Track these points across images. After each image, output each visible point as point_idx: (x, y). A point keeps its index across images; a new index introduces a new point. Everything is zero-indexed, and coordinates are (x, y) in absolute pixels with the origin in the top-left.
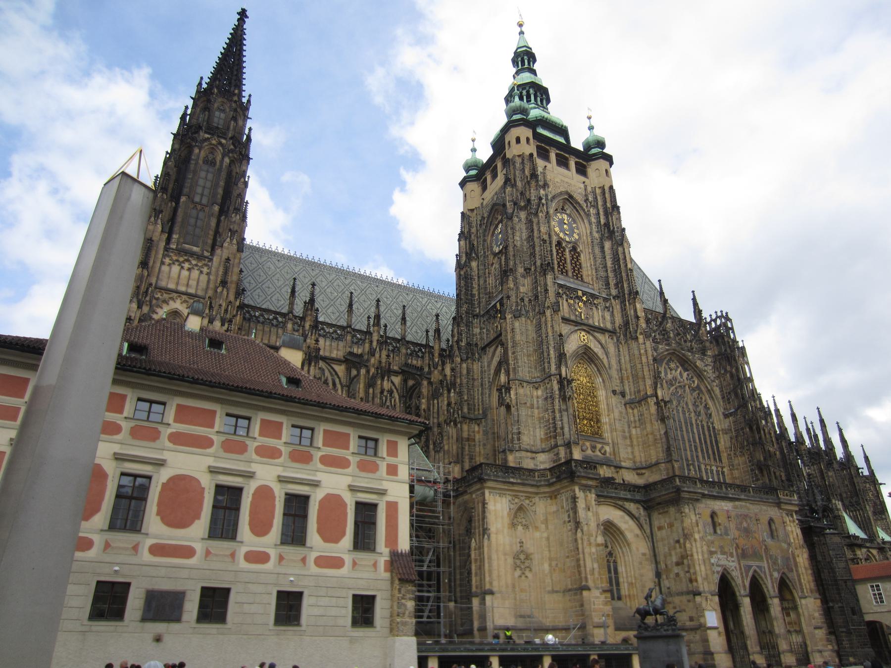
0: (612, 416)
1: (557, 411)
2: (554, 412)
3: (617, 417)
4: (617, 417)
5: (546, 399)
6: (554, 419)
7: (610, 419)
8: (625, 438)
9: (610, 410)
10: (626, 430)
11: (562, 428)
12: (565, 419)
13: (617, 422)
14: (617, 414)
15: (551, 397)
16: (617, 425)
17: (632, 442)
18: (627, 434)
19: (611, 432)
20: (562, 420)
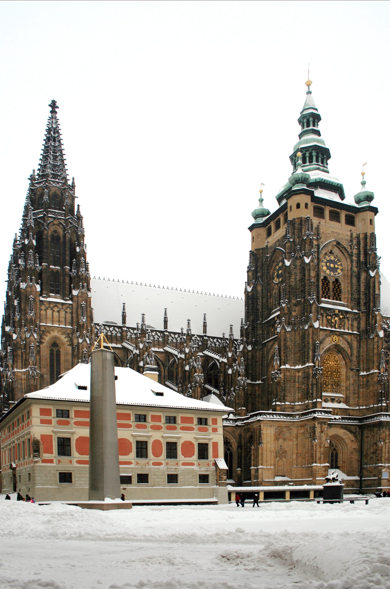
0: (348, 382)
1: (310, 385)
2: (308, 385)
3: (351, 383)
4: (351, 383)
5: (304, 378)
6: (308, 388)
7: (346, 384)
8: (355, 393)
9: (347, 378)
10: (356, 389)
11: (312, 394)
12: (315, 389)
13: (351, 385)
14: (352, 380)
15: (307, 377)
16: (351, 387)
17: (359, 395)
18: (356, 392)
19: (346, 391)
20: (312, 390)
